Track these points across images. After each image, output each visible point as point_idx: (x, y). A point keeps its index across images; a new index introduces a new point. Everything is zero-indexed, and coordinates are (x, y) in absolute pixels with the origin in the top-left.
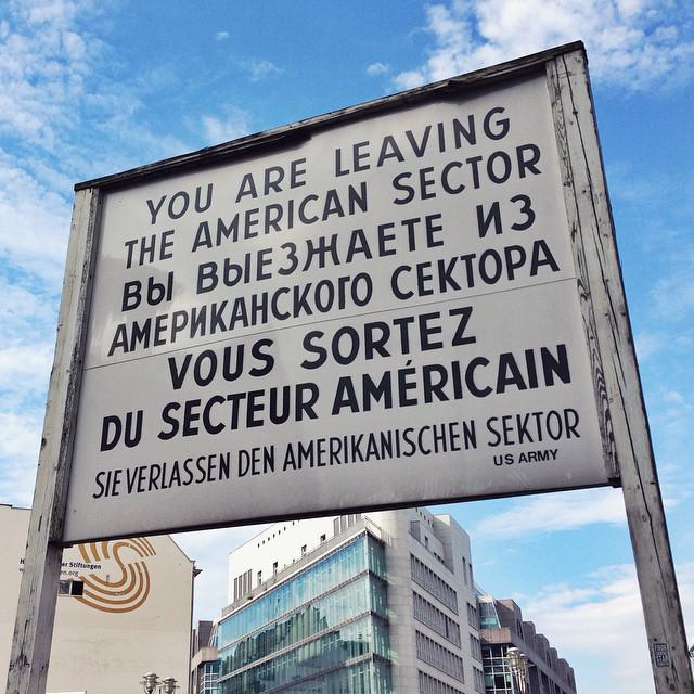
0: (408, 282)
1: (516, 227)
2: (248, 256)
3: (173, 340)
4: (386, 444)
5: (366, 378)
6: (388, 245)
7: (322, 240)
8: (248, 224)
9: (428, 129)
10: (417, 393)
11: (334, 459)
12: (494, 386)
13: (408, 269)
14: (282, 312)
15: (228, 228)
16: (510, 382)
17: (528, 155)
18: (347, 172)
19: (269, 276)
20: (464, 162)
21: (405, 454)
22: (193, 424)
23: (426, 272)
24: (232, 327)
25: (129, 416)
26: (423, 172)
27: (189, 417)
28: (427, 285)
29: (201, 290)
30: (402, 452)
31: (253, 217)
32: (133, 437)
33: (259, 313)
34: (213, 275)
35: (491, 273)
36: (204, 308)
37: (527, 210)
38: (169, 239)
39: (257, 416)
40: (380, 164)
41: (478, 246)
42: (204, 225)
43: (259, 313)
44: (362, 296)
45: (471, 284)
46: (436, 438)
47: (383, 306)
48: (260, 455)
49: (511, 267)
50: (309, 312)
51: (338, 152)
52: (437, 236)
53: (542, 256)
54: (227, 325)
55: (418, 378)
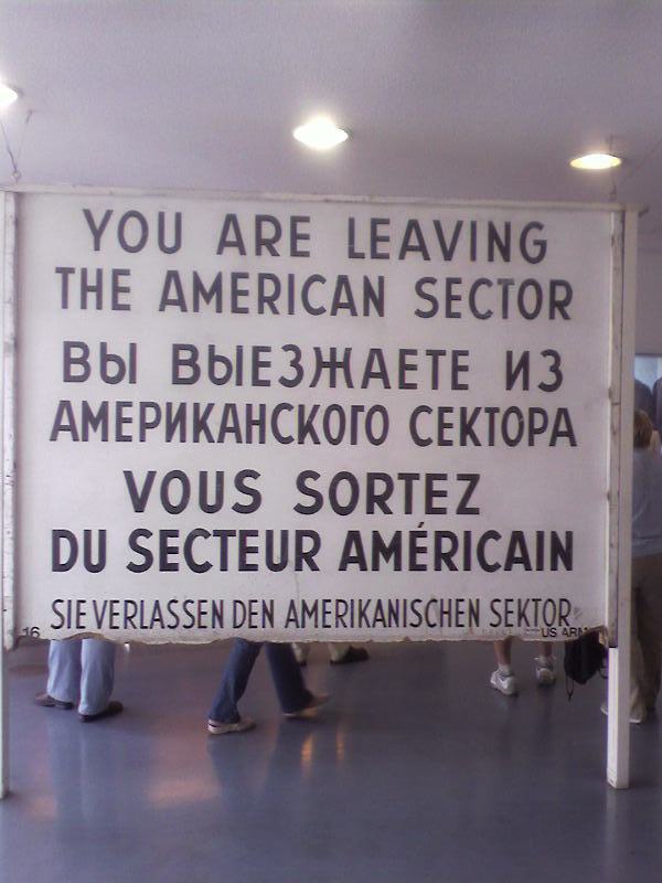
0: (428, 426)
1: (543, 387)
2: (240, 350)
3: (142, 440)
4: (393, 613)
5: (376, 536)
6: (410, 377)
7: (333, 351)
8: (236, 293)
9: (459, 225)
10: (426, 559)
11: (340, 622)
12: (502, 562)
13: (428, 410)
14: (284, 434)
15: (208, 291)
16: (518, 561)
17: (561, 294)
18: (362, 256)
19: (267, 383)
20: (495, 281)
21: (412, 625)
22: (171, 559)
23: (448, 418)
24: (221, 440)
25: (88, 533)
26: (451, 282)
27: (166, 550)
28: (449, 434)
29: (177, 380)
30: (408, 625)
31: (242, 285)
32: (95, 561)
33: (256, 429)
34: (192, 362)
35: (513, 435)
36: (183, 406)
37: (555, 369)
38: (123, 281)
39: (251, 559)
40: (402, 257)
41: (502, 399)
42: (173, 276)
43: (256, 429)
44: (377, 434)
45: (491, 443)
46: (443, 613)
47: (398, 455)
48: (257, 608)
49: (533, 432)
50: (317, 442)
51: (352, 222)
52: (462, 378)
53: (563, 427)
54: (215, 436)
55: (428, 543)
